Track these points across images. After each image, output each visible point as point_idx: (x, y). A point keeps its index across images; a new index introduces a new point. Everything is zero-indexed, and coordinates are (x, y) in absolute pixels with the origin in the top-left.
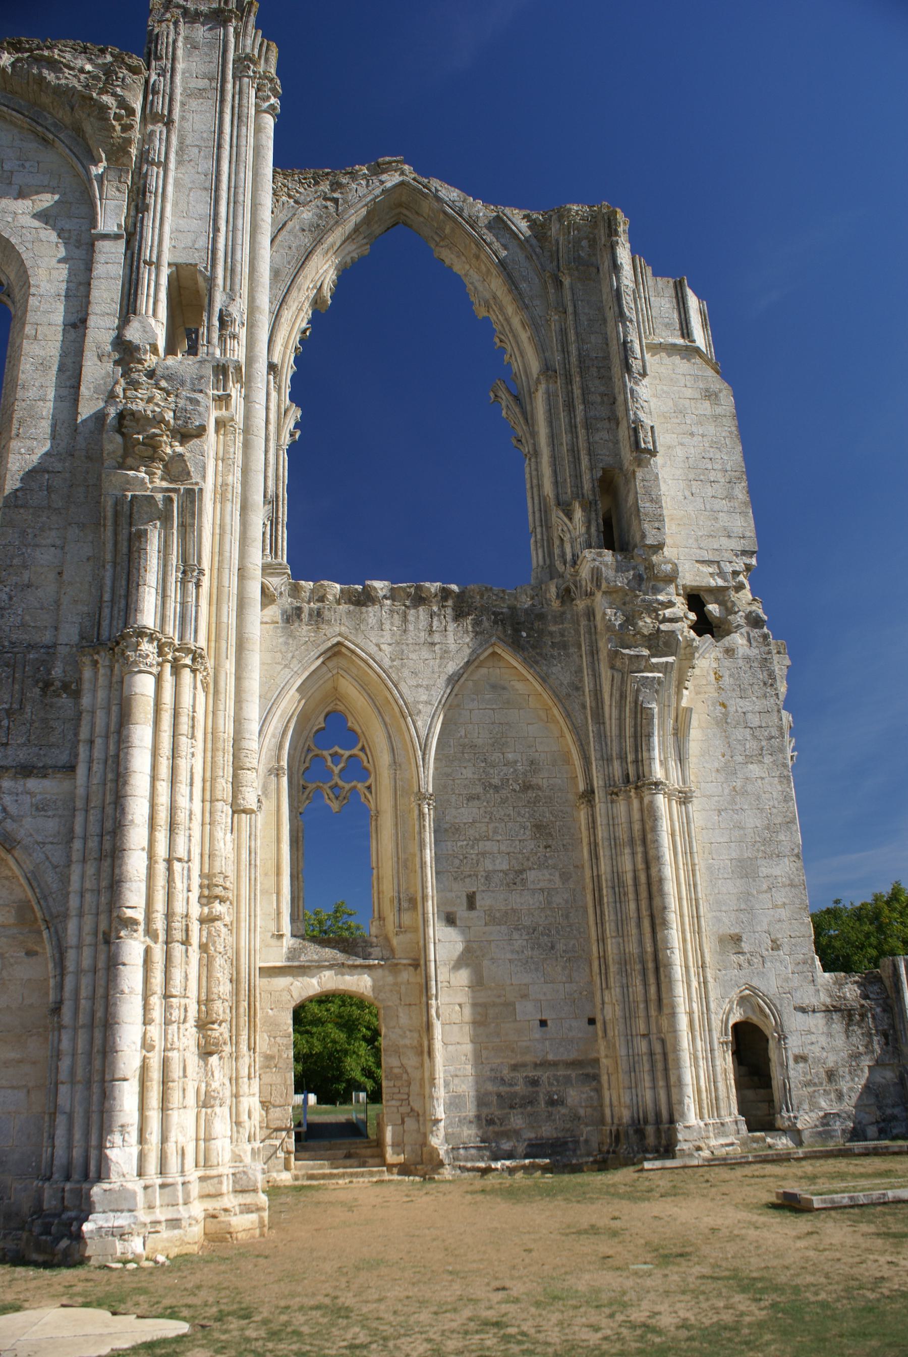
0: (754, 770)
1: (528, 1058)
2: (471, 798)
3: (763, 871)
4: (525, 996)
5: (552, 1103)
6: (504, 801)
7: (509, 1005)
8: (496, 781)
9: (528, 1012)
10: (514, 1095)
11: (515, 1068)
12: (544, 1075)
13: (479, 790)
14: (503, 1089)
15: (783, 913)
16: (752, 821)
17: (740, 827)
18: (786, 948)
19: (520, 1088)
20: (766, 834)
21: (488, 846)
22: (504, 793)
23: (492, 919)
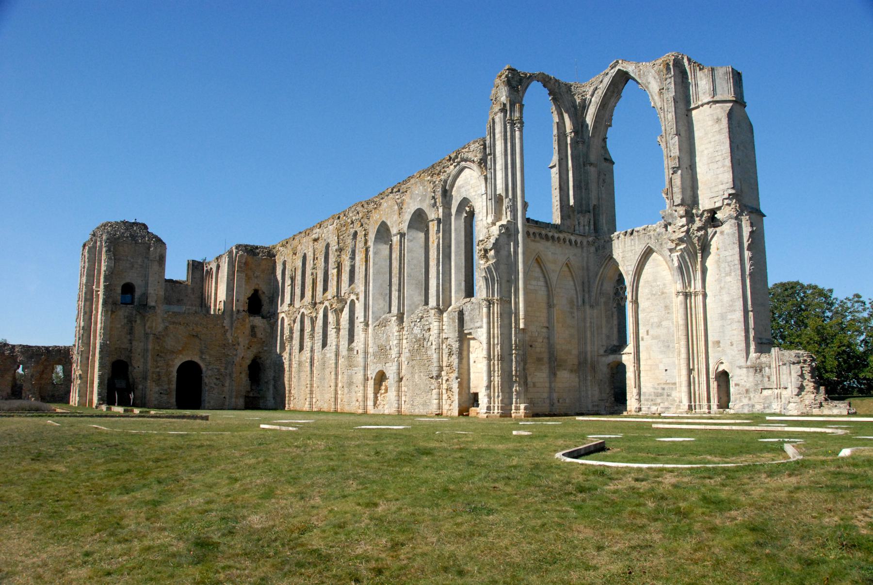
0: (728, 279)
1: (662, 382)
2: (648, 299)
3: (729, 317)
4: (661, 362)
5: (668, 396)
6: (656, 299)
7: (657, 365)
8: (654, 292)
9: (662, 367)
10: (658, 393)
11: (658, 384)
12: (666, 387)
13: (650, 296)
14: (656, 391)
15: (735, 332)
16: (726, 298)
17: (722, 301)
18: (735, 346)
19: (660, 391)
20: (731, 303)
21: (652, 314)
22: (657, 296)
23: (654, 338)
